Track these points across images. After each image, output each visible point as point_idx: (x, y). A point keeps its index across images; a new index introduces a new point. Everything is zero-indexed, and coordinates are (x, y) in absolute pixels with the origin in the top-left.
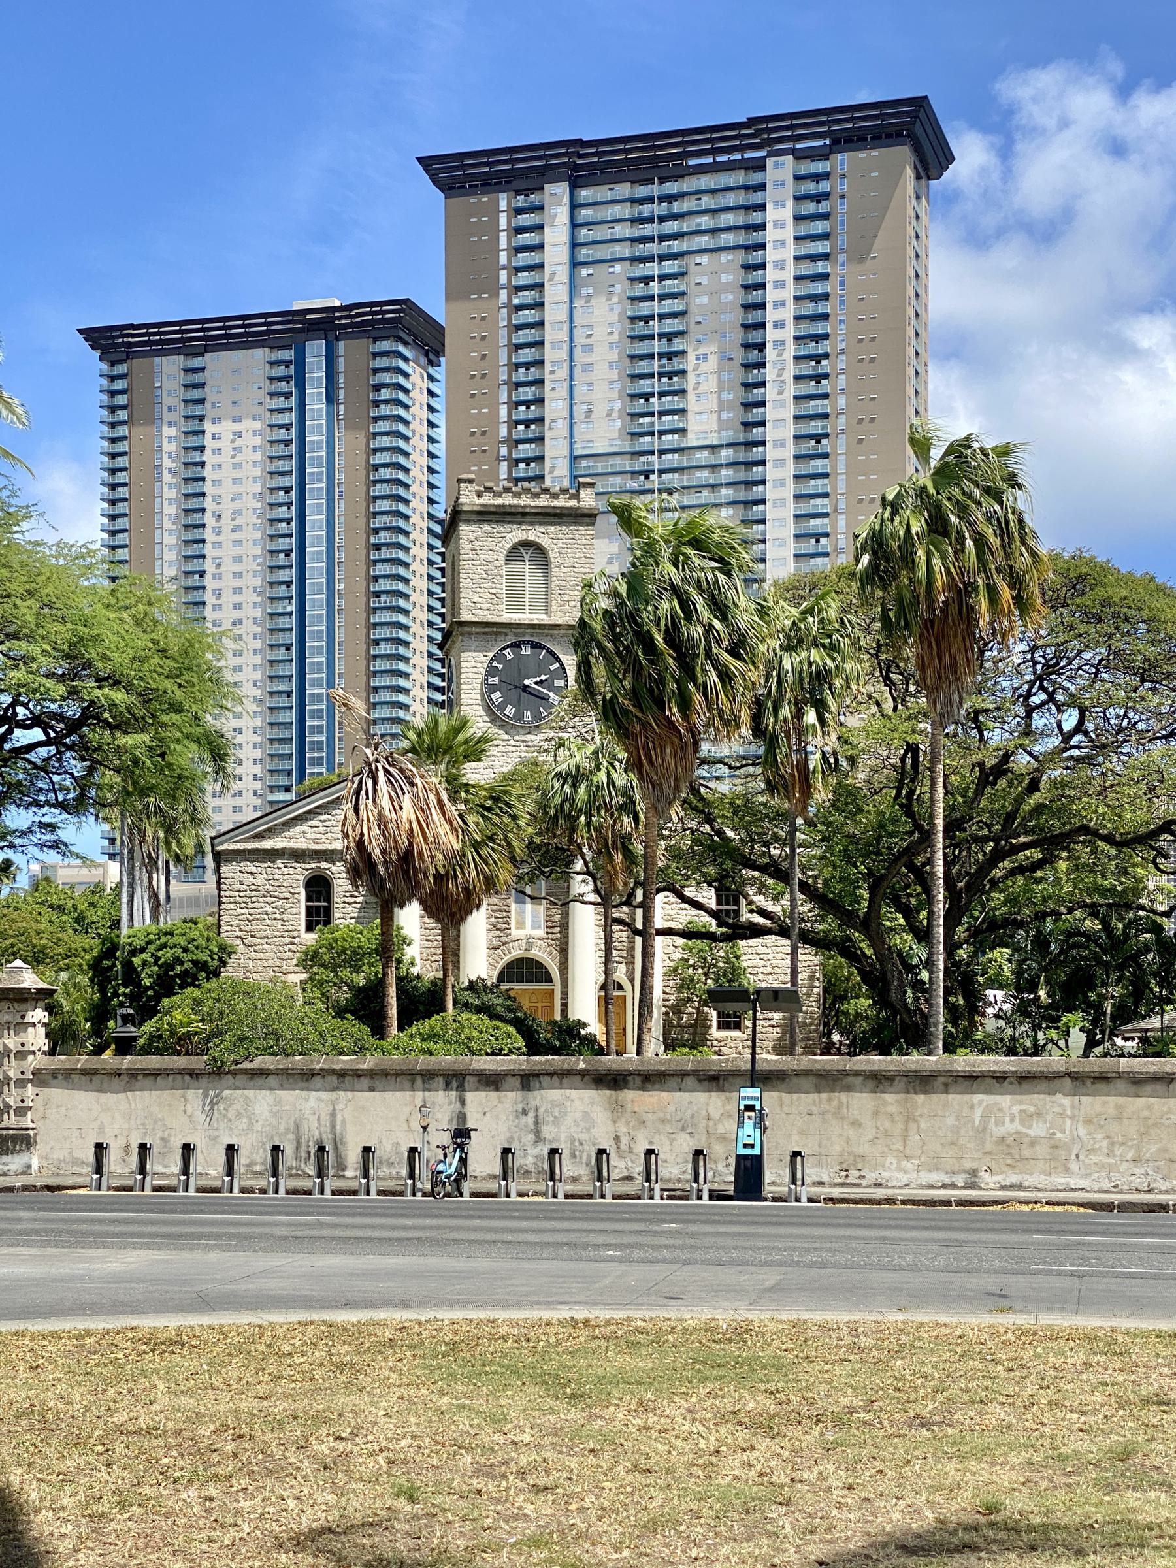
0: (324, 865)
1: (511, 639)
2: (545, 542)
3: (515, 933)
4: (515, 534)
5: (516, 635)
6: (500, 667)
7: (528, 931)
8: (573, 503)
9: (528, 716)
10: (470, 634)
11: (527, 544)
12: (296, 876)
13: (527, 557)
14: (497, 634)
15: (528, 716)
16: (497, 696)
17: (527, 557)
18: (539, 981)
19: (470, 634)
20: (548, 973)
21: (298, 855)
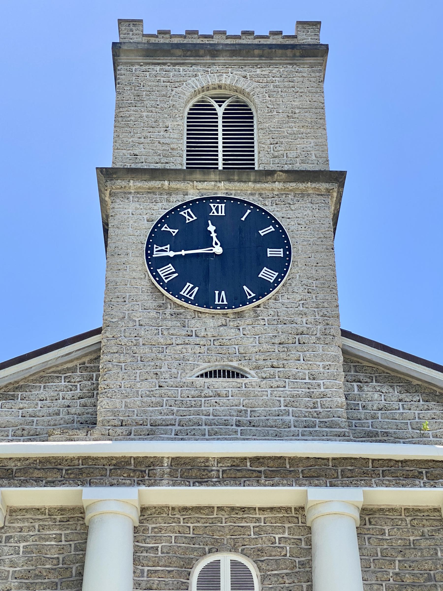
9: (221, 297)
15: (221, 297)
16: (167, 271)
17: (220, 111)
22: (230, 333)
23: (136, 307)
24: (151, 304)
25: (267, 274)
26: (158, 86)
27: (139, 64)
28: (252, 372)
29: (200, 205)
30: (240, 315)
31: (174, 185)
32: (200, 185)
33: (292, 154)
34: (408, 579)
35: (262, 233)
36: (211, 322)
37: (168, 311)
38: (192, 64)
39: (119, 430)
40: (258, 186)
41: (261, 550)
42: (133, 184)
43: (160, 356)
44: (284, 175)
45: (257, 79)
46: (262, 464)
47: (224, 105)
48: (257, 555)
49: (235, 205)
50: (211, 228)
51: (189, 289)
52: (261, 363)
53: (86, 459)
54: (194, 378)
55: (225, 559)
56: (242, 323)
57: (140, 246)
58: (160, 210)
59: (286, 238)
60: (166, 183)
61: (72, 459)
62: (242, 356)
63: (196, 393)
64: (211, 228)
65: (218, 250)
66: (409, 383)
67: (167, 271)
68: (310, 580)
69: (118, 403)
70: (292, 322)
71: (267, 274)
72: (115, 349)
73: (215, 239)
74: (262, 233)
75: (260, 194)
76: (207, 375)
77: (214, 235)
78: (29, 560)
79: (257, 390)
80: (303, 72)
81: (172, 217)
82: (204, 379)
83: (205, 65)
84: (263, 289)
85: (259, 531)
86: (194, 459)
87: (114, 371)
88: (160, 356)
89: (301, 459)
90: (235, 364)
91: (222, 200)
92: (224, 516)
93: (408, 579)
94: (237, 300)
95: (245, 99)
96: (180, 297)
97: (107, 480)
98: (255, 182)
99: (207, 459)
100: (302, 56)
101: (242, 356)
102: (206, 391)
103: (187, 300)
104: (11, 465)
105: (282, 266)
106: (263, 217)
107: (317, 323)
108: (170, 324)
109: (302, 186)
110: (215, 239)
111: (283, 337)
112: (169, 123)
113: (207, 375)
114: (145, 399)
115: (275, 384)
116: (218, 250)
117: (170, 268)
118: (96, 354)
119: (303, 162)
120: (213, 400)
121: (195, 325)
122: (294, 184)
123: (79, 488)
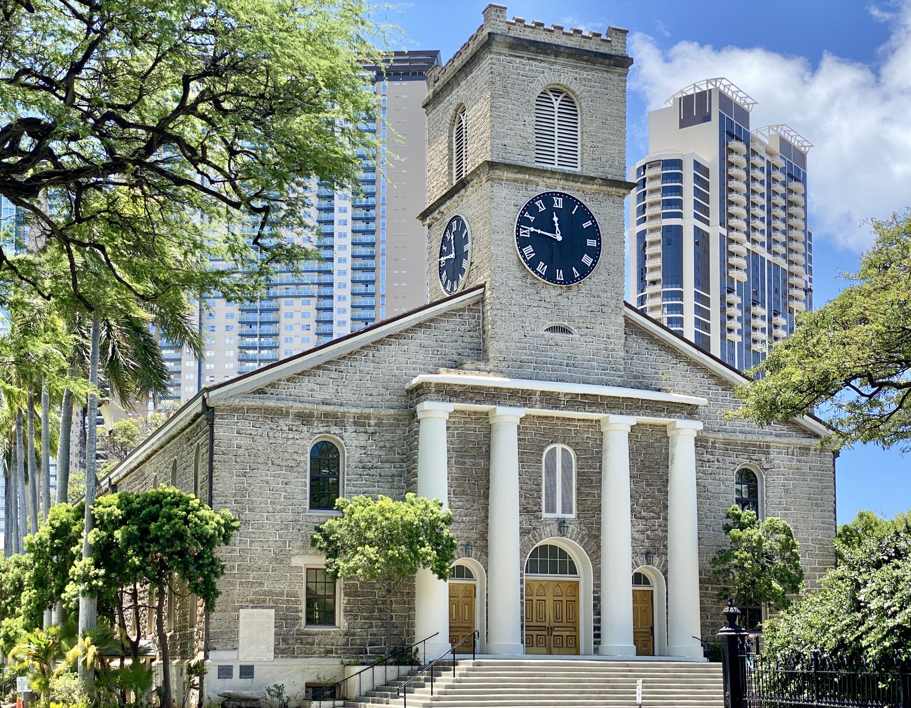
0: (334, 429)
1: (542, 189)
3: (545, 515)
6: (532, 218)
7: (559, 514)
11: (557, 92)
12: (304, 443)
14: (527, 182)
18: (563, 572)
20: (572, 563)
21: (305, 418)
22: (563, 301)
23: (510, 276)
25: (587, 260)
26: (518, 79)
27: (505, 55)
28: (576, 331)
29: (547, 198)
30: (569, 288)
31: (531, 178)
32: (547, 180)
33: (604, 159)
34: (647, 464)
35: (585, 225)
36: (554, 292)
37: (529, 281)
38: (542, 61)
39: (503, 364)
40: (584, 186)
41: (577, 443)
42: (507, 175)
43: (525, 314)
44: (601, 181)
45: (584, 83)
46: (587, 399)
47: (560, 99)
48: (575, 446)
49: (570, 201)
50: (555, 219)
51: (542, 267)
52: (581, 325)
53: (496, 388)
54: (543, 332)
55: (559, 447)
56: (571, 294)
57: (511, 227)
58: (524, 202)
59: (599, 232)
60: (527, 176)
61: (489, 388)
62: (570, 319)
63: (546, 343)
64: (555, 219)
65: (559, 238)
66: (652, 337)
68: (601, 462)
69: (502, 345)
70: (598, 296)
71: (587, 260)
72: (499, 306)
73: (557, 229)
74: (585, 225)
75: (583, 191)
76: (552, 329)
77: (557, 225)
78: (461, 441)
79: (579, 344)
80: (613, 77)
81: (530, 207)
82: (548, 334)
83: (549, 63)
84: (585, 271)
85: (577, 432)
86: (553, 393)
87: (499, 323)
88: (525, 314)
89: (607, 397)
90: (566, 323)
91: (561, 195)
92: (559, 422)
93: (647, 464)
94: (569, 279)
95: (573, 97)
96: (537, 272)
97: (508, 402)
98: (582, 183)
99: (559, 393)
100: (616, 66)
101: (570, 319)
102: (551, 342)
103: (541, 275)
104: (456, 388)
105: (595, 253)
106: (586, 214)
107: (612, 298)
108: (530, 291)
109: (610, 189)
110: (557, 229)
111: (593, 308)
112: (526, 118)
113: (552, 329)
114: (518, 344)
115: (588, 340)
116: (559, 238)
117: (530, 249)
118: (481, 301)
119: (611, 166)
120: (555, 348)
121: (544, 293)
122: (605, 188)
123: (494, 406)
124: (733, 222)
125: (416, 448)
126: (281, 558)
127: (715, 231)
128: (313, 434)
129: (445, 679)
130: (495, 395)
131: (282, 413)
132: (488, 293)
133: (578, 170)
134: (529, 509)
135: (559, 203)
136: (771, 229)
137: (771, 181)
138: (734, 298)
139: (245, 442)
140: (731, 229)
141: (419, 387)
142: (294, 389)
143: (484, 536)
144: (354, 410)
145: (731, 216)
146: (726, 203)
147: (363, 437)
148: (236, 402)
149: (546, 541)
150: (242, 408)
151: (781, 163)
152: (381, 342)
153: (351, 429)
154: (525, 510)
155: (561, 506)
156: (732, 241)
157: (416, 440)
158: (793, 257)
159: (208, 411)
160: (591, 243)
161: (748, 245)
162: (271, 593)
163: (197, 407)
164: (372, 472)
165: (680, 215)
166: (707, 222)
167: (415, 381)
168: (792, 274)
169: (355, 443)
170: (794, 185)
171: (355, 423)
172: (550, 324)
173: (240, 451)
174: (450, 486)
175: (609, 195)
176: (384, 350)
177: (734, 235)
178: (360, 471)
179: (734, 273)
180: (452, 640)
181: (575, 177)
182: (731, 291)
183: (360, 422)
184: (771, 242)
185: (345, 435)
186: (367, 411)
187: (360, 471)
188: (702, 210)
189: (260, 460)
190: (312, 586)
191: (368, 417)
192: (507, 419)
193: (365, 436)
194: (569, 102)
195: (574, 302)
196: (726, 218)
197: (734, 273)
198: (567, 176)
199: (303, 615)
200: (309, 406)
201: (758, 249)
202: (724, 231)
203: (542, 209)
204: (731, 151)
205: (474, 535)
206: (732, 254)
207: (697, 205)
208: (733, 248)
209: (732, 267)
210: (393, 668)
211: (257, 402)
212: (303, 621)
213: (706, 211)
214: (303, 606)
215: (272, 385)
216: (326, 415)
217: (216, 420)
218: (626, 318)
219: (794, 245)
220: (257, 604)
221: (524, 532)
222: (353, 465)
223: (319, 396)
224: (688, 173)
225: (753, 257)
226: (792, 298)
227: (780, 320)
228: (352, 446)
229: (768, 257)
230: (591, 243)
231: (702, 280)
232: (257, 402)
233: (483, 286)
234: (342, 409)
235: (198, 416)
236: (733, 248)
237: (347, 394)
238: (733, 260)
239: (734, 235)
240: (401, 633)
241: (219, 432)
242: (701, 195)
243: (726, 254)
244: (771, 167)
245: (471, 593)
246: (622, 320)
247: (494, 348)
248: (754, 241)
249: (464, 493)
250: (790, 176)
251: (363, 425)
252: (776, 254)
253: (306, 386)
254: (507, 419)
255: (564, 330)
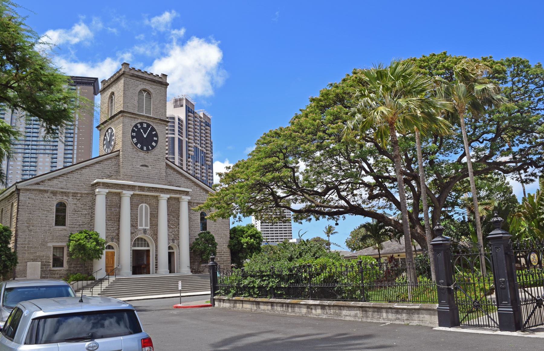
0: (65, 198)
1: (140, 121)
2: (151, 90)
3: (139, 227)
4: (143, 85)
5: (141, 120)
7: (144, 227)
8: (160, 80)
9: (145, 148)
10: (126, 116)
11: (145, 90)
13: (145, 95)
14: (135, 118)
15: (145, 148)
16: (135, 140)
17: (145, 95)
19: (126, 116)
21: (54, 193)
24: (131, 147)
25: (154, 144)
29: (141, 124)
36: (143, 154)
48: (149, 204)
49: (148, 125)
55: (144, 205)
58: (134, 124)
62: (148, 162)
65: (145, 136)
67: (135, 140)
71: (154, 144)
81: (136, 126)
84: (153, 147)
91: (146, 123)
105: (156, 142)
116: (145, 136)
124: (190, 137)
125: (95, 204)
126: (44, 244)
127: (184, 139)
128: (57, 199)
129: (105, 284)
130: (123, 187)
131: (46, 191)
132: (121, 153)
133: (151, 116)
134: (134, 225)
135: (145, 125)
136: (201, 140)
137: (201, 125)
138: (190, 160)
139: (32, 202)
140: (189, 139)
141: (97, 183)
142: (50, 183)
143: (118, 235)
144: (72, 191)
145: (189, 135)
146: (187, 131)
147: (75, 200)
148: (29, 187)
149: (139, 236)
150: (31, 190)
151: (204, 121)
152: (83, 168)
153: (71, 198)
154: (132, 226)
155: (144, 224)
156: (189, 143)
157: (95, 202)
158: (208, 148)
159: (18, 190)
160: (155, 139)
161: (194, 144)
162: (39, 256)
163: (13, 189)
164: (78, 213)
165: (174, 134)
166: (182, 137)
167: (95, 181)
168: (207, 154)
169: (73, 202)
170: (207, 127)
171: (73, 196)
172: (142, 164)
173: (29, 205)
174: (106, 218)
175: (161, 124)
176: (84, 171)
177: (190, 141)
178: (74, 212)
179: (190, 152)
180: (107, 271)
181: (150, 118)
182: (189, 158)
183: (75, 195)
184: (201, 143)
185: (69, 200)
186: (77, 191)
187: (74, 212)
188: (180, 133)
189: (37, 208)
190: (55, 254)
191: (77, 193)
192: (127, 194)
193: (76, 200)
194: (149, 93)
195: (150, 157)
196: (188, 135)
197: (190, 152)
198: (148, 117)
199: (51, 264)
200: (56, 189)
201: (197, 145)
202: (187, 140)
203: (139, 127)
204: (189, 116)
205: (114, 234)
206: (189, 146)
207: (179, 131)
208: (190, 144)
209: (189, 150)
210: (86, 282)
211: (36, 187)
212: (51, 266)
213: (182, 133)
214: (51, 261)
215: (42, 182)
216: (62, 192)
217: (21, 194)
218: (166, 163)
219: (208, 145)
220: (34, 260)
221: (132, 233)
222: (71, 210)
223: (60, 186)
224: (177, 121)
225: (196, 148)
226: (207, 161)
227: (204, 167)
228: (71, 204)
229: (200, 148)
230: (155, 139)
231: (181, 154)
232: (36, 187)
233: (119, 151)
234: (68, 191)
235: (13, 192)
236: (190, 144)
237: (69, 185)
238: (190, 148)
239: (190, 141)
240: (88, 269)
241: (21, 198)
242: (180, 128)
243: (188, 146)
244: (201, 122)
245: (113, 254)
246: (165, 164)
247: (122, 170)
248: (196, 143)
249: (111, 220)
250: (206, 125)
251: (76, 196)
252: (202, 147)
253: (55, 181)
254: (127, 194)
255: (146, 166)
